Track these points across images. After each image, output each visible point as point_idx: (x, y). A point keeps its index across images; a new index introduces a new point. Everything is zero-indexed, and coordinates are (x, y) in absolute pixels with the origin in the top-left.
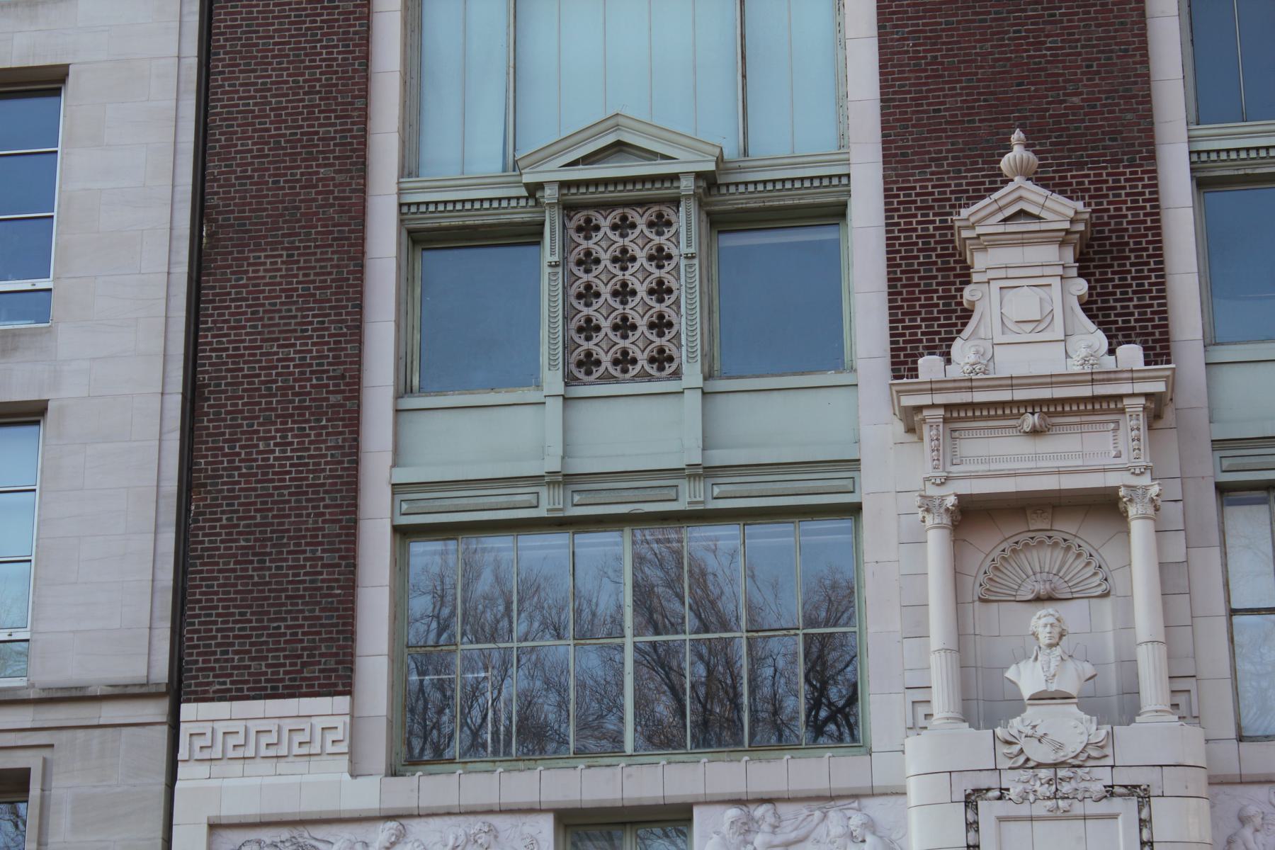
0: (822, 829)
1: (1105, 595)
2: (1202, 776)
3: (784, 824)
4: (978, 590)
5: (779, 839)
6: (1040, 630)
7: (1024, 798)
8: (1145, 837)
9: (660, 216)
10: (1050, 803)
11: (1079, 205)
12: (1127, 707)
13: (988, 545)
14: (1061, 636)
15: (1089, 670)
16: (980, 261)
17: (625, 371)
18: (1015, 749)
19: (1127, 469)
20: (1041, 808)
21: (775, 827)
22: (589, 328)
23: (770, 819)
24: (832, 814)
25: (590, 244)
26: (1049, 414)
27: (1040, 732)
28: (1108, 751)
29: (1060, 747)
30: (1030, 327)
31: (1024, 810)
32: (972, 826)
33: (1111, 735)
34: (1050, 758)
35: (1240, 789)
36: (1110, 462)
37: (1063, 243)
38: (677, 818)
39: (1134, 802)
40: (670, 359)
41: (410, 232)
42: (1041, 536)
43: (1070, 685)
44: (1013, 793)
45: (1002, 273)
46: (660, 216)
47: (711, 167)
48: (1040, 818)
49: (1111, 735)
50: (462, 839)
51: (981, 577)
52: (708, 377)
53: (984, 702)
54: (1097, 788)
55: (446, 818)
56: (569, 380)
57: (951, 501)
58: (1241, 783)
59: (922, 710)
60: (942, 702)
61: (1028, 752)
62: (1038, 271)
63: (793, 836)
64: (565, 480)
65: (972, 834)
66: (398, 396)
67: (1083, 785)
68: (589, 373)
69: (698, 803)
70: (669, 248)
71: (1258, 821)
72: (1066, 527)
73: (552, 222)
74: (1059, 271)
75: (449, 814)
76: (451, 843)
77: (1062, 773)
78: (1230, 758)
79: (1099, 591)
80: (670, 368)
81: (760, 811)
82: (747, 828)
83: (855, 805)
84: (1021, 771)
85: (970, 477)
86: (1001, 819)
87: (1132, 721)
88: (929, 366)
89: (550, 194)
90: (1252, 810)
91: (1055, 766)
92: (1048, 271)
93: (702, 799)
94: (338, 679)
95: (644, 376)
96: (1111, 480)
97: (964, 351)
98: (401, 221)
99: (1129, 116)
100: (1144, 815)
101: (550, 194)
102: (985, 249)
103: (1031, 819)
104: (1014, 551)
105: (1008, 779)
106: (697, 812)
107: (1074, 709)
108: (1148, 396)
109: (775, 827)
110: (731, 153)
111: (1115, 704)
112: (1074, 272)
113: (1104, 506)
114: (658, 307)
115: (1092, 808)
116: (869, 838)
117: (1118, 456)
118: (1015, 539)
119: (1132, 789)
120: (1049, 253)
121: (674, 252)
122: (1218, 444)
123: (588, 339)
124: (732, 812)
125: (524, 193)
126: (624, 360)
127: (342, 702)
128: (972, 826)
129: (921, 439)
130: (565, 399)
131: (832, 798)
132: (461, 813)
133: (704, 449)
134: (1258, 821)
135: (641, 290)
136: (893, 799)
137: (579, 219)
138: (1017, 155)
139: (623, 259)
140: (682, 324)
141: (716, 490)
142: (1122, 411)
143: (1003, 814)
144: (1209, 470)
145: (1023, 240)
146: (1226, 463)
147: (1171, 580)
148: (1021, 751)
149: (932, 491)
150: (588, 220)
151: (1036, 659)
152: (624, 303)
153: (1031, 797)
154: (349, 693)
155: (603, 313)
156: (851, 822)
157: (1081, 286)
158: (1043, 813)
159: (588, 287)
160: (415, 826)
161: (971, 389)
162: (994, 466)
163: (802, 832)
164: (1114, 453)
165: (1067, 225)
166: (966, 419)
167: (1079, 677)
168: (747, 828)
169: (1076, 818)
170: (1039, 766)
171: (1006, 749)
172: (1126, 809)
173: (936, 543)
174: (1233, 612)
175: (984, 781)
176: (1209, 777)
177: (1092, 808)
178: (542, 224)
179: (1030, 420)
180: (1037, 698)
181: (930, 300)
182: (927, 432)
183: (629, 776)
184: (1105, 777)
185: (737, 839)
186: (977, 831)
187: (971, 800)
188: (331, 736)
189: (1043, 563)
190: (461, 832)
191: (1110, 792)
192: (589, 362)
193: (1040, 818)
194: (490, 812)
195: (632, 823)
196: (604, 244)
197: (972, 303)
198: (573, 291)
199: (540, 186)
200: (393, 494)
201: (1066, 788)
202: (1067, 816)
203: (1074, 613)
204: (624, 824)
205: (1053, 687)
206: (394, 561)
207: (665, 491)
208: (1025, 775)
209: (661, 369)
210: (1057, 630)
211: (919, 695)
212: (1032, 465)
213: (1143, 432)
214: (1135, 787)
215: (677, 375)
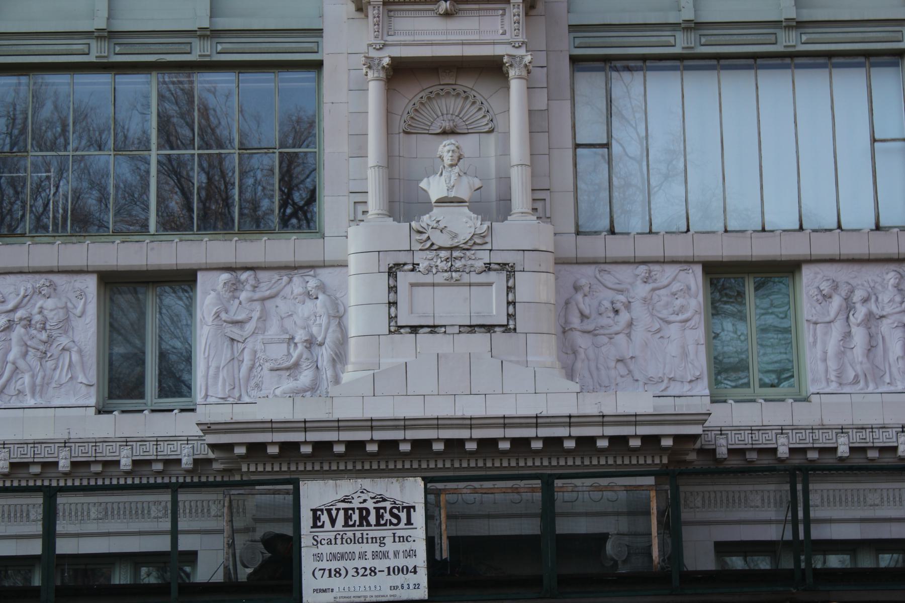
0: (288, 289)
1: (491, 131)
2: (551, 257)
3: (262, 285)
5: (258, 295)
6: (445, 154)
7: (429, 270)
8: (511, 298)
10: (446, 275)
12: (502, 208)
13: (411, 94)
14: (459, 159)
15: (477, 183)
18: (424, 237)
19: (510, 43)
20: (440, 278)
21: (255, 287)
23: (252, 281)
24: (296, 280)
27: (442, 225)
28: (488, 239)
29: (456, 236)
31: (429, 279)
32: (393, 289)
33: (490, 229)
34: (448, 243)
35: (576, 268)
36: (498, 37)
38: (184, 279)
42: (449, 88)
43: (464, 192)
44: (421, 267)
48: (439, 285)
49: (490, 229)
50: (30, 291)
51: (405, 115)
53: (404, 203)
54: (480, 264)
55: (19, 276)
57: (386, 61)
58: (577, 263)
59: (360, 208)
60: (374, 203)
61: (434, 239)
63: (267, 293)
64: (109, 35)
65: (392, 294)
67: (470, 262)
69: (201, 269)
71: (586, 289)
72: (466, 83)
75: (21, 273)
76: (22, 293)
77: (456, 254)
78: (570, 246)
79: (486, 129)
81: (244, 276)
82: (235, 288)
83: (312, 273)
84: (428, 252)
85: (400, 45)
86: (413, 285)
87: (506, 219)
90: (583, 281)
91: (451, 249)
93: (204, 267)
96: (499, 51)
100: (510, 284)
103: (434, 285)
104: (429, 98)
105: (419, 258)
106: (200, 276)
107: (466, 210)
109: (255, 287)
111: (494, 206)
113: (492, 69)
115: (475, 278)
116: (321, 296)
117: (504, 33)
118: (430, 90)
119: (503, 266)
122: (573, 28)
124: (225, 276)
128: (393, 289)
129: (367, 16)
131: (295, 268)
132: (29, 273)
133: (211, 17)
134: (586, 289)
136: (338, 269)
141: (219, 47)
143: (413, 281)
144: (566, 46)
146: (578, 41)
147: (537, 122)
148: (429, 238)
149: (373, 54)
151: (441, 174)
153: (434, 270)
156: (309, 285)
158: (442, 281)
162: (417, 38)
163: (273, 291)
164: (501, 32)
167: (470, 187)
168: (235, 288)
169: (464, 285)
170: (441, 248)
171: (418, 237)
172: (499, 279)
173: (374, 91)
174: (577, 146)
175: (402, 258)
176: (555, 259)
177: (475, 278)
180: (441, 201)
182: (371, 12)
183: (152, 249)
184: (485, 257)
185: (228, 295)
186: (396, 293)
187: (393, 271)
189: (448, 109)
190: (29, 286)
191: (488, 268)
193: (439, 285)
194: (51, 272)
195: (153, 282)
201: (458, 264)
202: (458, 283)
203: (468, 143)
204: (148, 283)
205: (452, 194)
207: (182, 46)
210: (457, 155)
211: (359, 198)
212: (444, 38)
214: (505, 264)
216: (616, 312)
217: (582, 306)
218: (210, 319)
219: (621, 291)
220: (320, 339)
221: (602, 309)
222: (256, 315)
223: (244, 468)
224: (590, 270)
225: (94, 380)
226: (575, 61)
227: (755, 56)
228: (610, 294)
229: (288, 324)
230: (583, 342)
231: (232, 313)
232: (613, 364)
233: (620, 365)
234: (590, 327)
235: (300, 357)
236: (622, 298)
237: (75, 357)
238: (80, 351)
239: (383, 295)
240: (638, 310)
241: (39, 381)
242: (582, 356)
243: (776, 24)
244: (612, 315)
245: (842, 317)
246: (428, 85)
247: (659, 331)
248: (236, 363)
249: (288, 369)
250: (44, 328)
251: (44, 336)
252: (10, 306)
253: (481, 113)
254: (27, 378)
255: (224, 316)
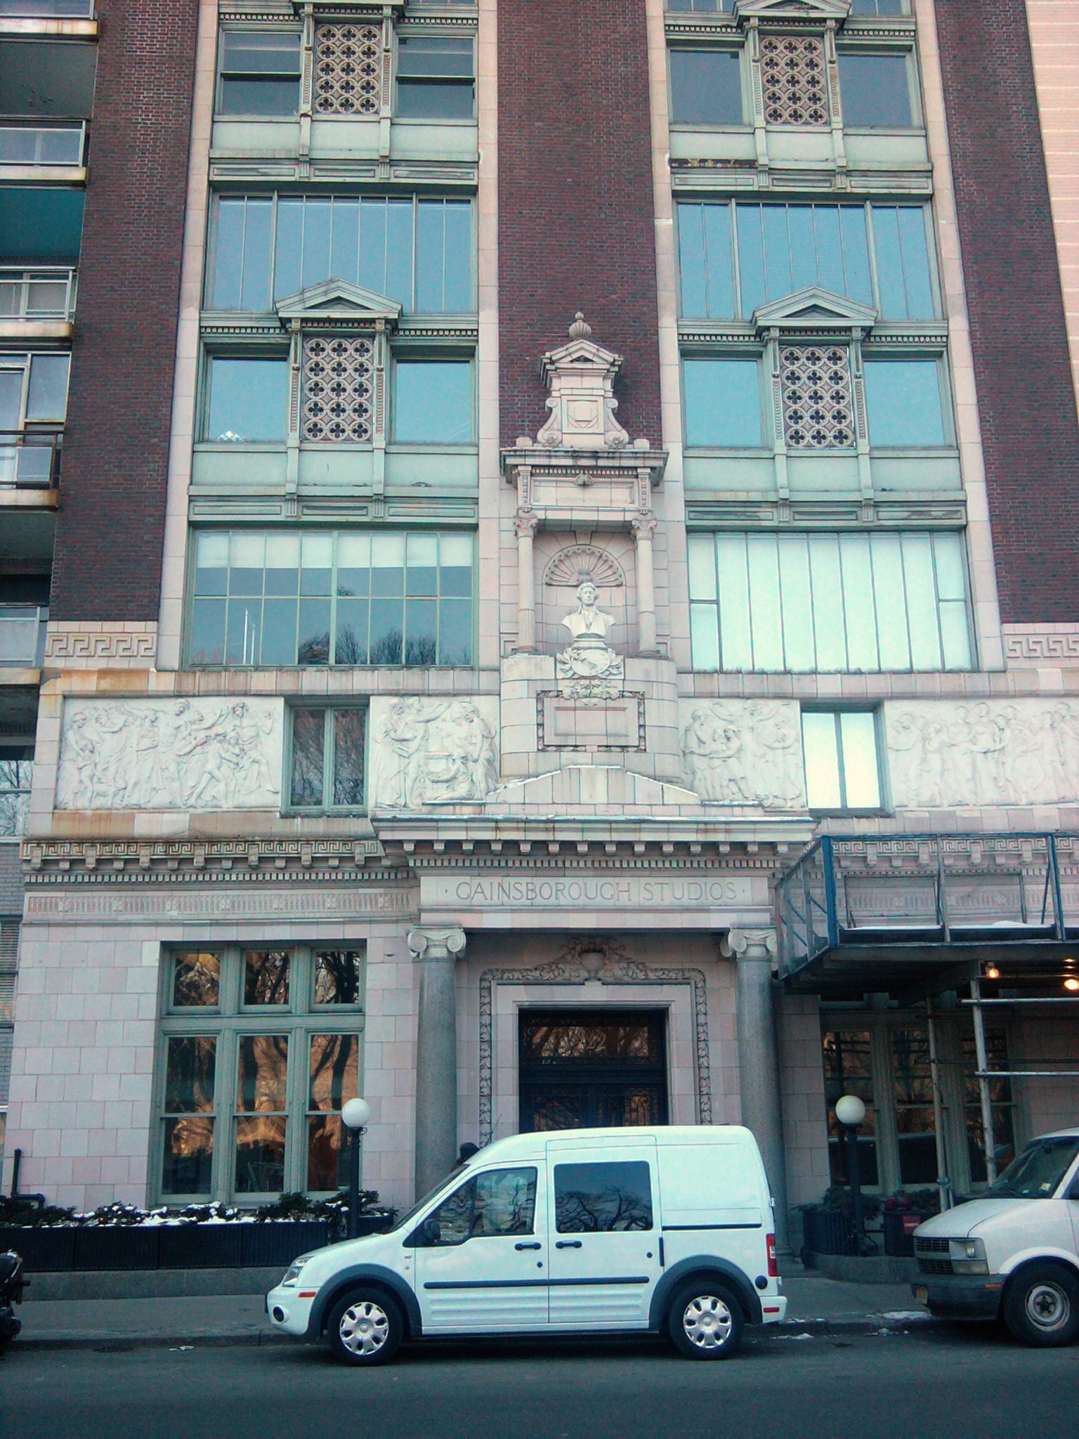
4: (546, 580)
9: (362, 345)
11: (616, 356)
13: (554, 550)
16: (556, 384)
17: (337, 436)
18: (567, 667)
22: (316, 409)
23: (417, 706)
25: (319, 359)
26: (593, 475)
29: (593, 666)
30: (583, 424)
31: (571, 704)
32: (540, 712)
35: (693, 700)
37: (605, 378)
39: (636, 700)
40: (366, 431)
41: (205, 344)
45: (569, 392)
46: (362, 345)
47: (396, 316)
52: (390, 443)
54: (615, 693)
56: (303, 440)
57: (534, 521)
62: (589, 392)
66: (194, 443)
68: (315, 436)
70: (367, 365)
72: (600, 545)
73: (296, 344)
74: (602, 392)
77: (596, 682)
80: (365, 437)
86: (558, 709)
88: (523, 442)
89: (295, 325)
92: (596, 392)
94: (150, 610)
95: (348, 440)
97: (542, 435)
98: (200, 337)
99: (645, 309)
101: (295, 325)
102: (559, 377)
103: (575, 709)
106: (372, 699)
108: (653, 468)
110: (409, 308)
112: (610, 395)
113: (624, 532)
114: (359, 400)
116: (476, 720)
119: (634, 694)
120: (597, 382)
121: (370, 367)
123: (315, 415)
125: (278, 324)
126: (337, 430)
127: (151, 626)
129: (516, 488)
130: (300, 450)
135: (350, 389)
137: (312, 343)
138: (579, 326)
139: (339, 369)
140: (373, 410)
142: (637, 477)
145: (582, 374)
150: (318, 345)
152: (338, 395)
154: (157, 620)
155: (326, 399)
157: (614, 403)
159: (317, 384)
160: (194, 702)
161: (550, 457)
165: (607, 366)
166: (543, 475)
168: (400, 710)
172: (631, 704)
173: (526, 543)
174: (692, 601)
178: (289, 345)
179: (583, 478)
181: (526, 401)
182: (520, 481)
187: (541, 696)
188: (143, 646)
192: (315, 430)
196: (328, 359)
197: (551, 409)
198: (307, 386)
199: (289, 320)
200: (190, 501)
206: (188, 547)
208: (573, 683)
209: (360, 436)
213: (648, 489)
215: (369, 440)
216: (728, 739)
217: (699, 734)
218: (380, 737)
219: (731, 722)
220: (475, 756)
221: (717, 736)
222: (420, 735)
223: (411, 864)
224: (706, 703)
225: (279, 788)
226: (690, 530)
227: (838, 531)
228: (723, 724)
229: (447, 742)
230: (698, 762)
231: (399, 732)
232: (725, 783)
233: (732, 784)
234: (707, 752)
235: (458, 770)
236: (732, 727)
237: (264, 768)
238: (268, 763)
239: (533, 719)
240: (747, 737)
241: (231, 789)
242: (699, 775)
243: (858, 504)
244: (724, 741)
245: (920, 745)
246: (567, 545)
247: (764, 755)
248: (402, 774)
249: (447, 781)
250: (237, 744)
251: (237, 751)
252: (207, 724)
253: (610, 572)
254: (222, 787)
255: (392, 734)
